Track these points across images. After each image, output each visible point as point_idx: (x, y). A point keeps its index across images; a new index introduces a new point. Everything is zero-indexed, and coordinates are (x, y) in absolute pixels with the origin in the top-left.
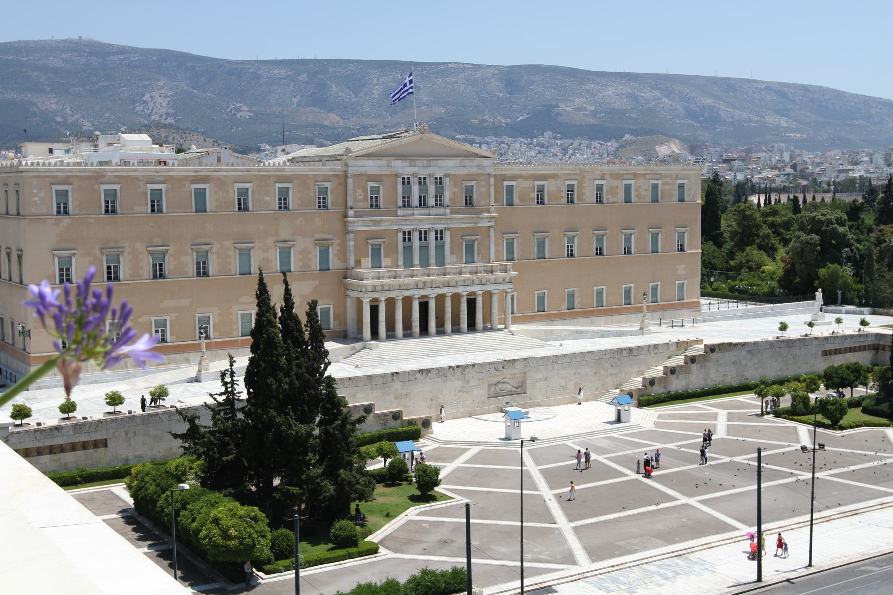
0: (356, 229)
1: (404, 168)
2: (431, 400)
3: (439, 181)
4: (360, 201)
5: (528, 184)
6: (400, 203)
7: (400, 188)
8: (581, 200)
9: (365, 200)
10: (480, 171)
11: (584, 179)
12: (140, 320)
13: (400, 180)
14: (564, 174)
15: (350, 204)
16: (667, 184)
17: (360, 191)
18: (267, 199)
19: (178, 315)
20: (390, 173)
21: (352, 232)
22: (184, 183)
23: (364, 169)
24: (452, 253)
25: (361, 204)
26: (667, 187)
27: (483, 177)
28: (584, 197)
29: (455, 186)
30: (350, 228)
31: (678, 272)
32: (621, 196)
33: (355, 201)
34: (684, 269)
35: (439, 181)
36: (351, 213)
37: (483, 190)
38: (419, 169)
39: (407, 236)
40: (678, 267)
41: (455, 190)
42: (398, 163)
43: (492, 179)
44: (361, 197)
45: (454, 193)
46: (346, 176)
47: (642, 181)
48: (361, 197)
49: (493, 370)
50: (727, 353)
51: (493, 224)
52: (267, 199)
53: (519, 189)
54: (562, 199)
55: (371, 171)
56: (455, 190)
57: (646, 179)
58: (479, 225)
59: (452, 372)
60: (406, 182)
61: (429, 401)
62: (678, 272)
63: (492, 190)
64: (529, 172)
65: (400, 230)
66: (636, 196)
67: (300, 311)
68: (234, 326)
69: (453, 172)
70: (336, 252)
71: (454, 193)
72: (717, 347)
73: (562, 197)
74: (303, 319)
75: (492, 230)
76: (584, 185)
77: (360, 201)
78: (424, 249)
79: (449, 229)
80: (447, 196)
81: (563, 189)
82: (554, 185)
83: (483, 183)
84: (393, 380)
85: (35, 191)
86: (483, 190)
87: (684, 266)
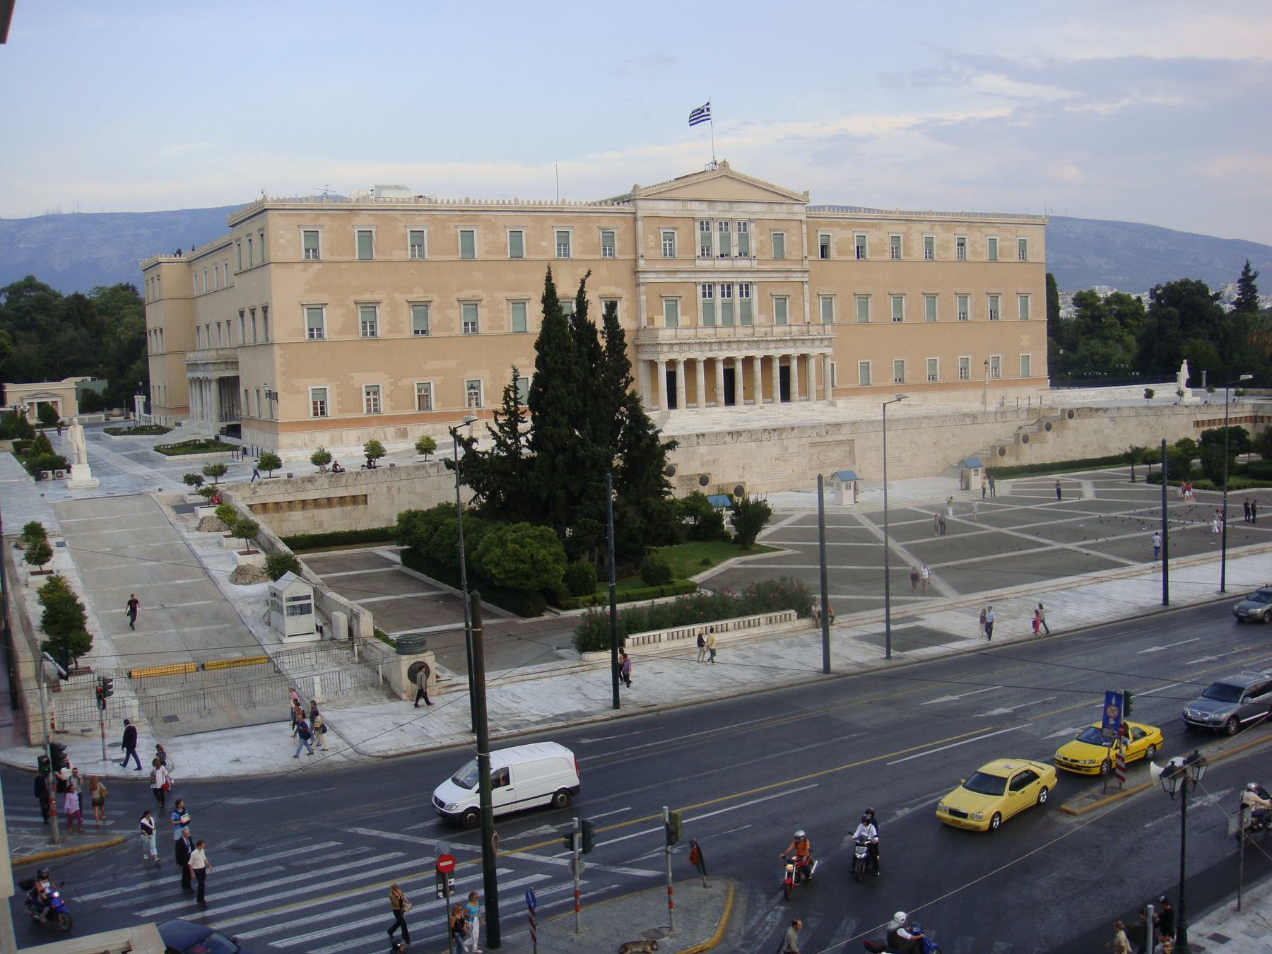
1: (702, 211)
2: (743, 468)
3: (743, 226)
4: (651, 248)
5: (847, 234)
6: (699, 252)
7: (698, 233)
9: (657, 247)
10: (791, 217)
12: (399, 384)
13: (698, 225)
15: (641, 252)
17: (651, 237)
18: (543, 244)
19: (443, 378)
21: (643, 284)
22: (448, 224)
24: (760, 312)
25: (653, 252)
27: (794, 224)
29: (761, 234)
30: (641, 280)
35: (743, 226)
36: (641, 263)
37: (794, 239)
38: (718, 212)
39: (708, 289)
41: (761, 238)
42: (695, 206)
43: (804, 227)
44: (652, 244)
46: (635, 219)
48: (652, 244)
50: (1086, 420)
51: (806, 279)
52: (543, 244)
53: (836, 240)
55: (662, 214)
56: (761, 238)
59: (767, 436)
60: (705, 225)
61: (741, 469)
63: (805, 237)
65: (699, 283)
67: (596, 315)
70: (625, 308)
71: (761, 242)
72: (1075, 411)
73: (886, 251)
74: (600, 325)
75: (806, 286)
77: (651, 248)
78: (728, 307)
80: (753, 244)
83: (795, 231)
84: (698, 443)
85: (280, 232)
86: (794, 239)
87: (1028, 336)
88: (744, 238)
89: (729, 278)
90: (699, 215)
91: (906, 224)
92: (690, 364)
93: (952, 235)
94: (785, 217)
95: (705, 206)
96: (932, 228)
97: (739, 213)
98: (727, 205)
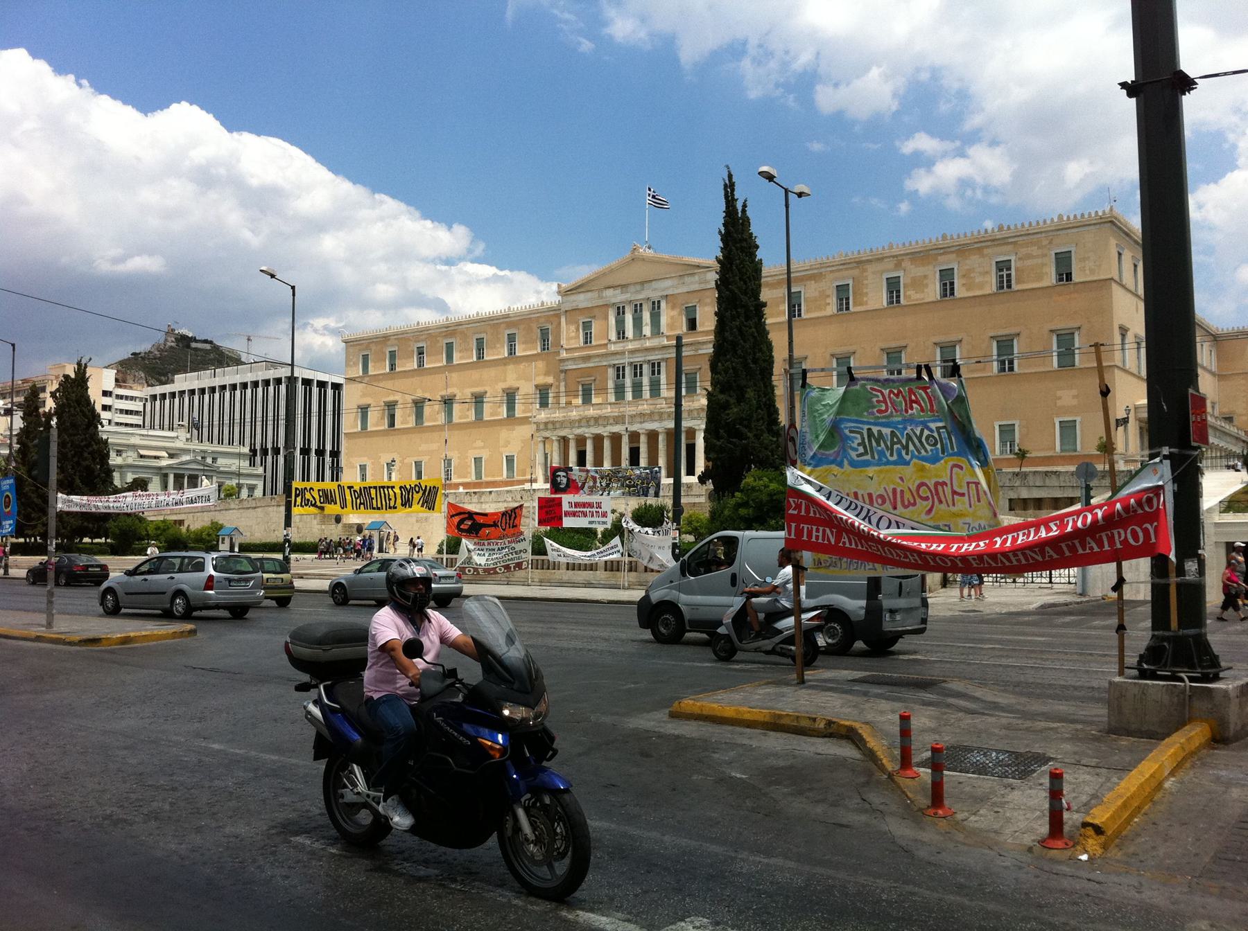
0: (566, 368)
1: (617, 297)
4: (572, 338)
6: (613, 336)
8: (861, 304)
10: (703, 286)
11: (865, 274)
14: (831, 271)
16: (1029, 256)
20: (601, 304)
23: (574, 304)
25: (573, 341)
26: (1029, 262)
28: (865, 299)
31: (1059, 403)
32: (933, 290)
33: (568, 339)
34: (1074, 397)
39: (620, 371)
40: (1059, 393)
42: (610, 292)
45: (672, 318)
47: (974, 261)
49: (510, 499)
54: (828, 307)
55: (582, 306)
57: (983, 256)
58: (700, 352)
59: (469, 498)
62: (1059, 403)
64: (776, 278)
65: (610, 366)
66: (964, 284)
68: (469, 470)
69: (670, 292)
71: (672, 318)
73: (829, 304)
76: (865, 282)
77: (572, 338)
79: (663, 359)
80: (664, 320)
81: (829, 292)
82: (815, 290)
87: (1074, 392)
88: (656, 317)
89: (638, 359)
90: (614, 301)
91: (858, 267)
92: (598, 440)
93: (931, 267)
94: (696, 287)
95: (618, 291)
96: (898, 266)
97: (652, 293)
98: (638, 287)
